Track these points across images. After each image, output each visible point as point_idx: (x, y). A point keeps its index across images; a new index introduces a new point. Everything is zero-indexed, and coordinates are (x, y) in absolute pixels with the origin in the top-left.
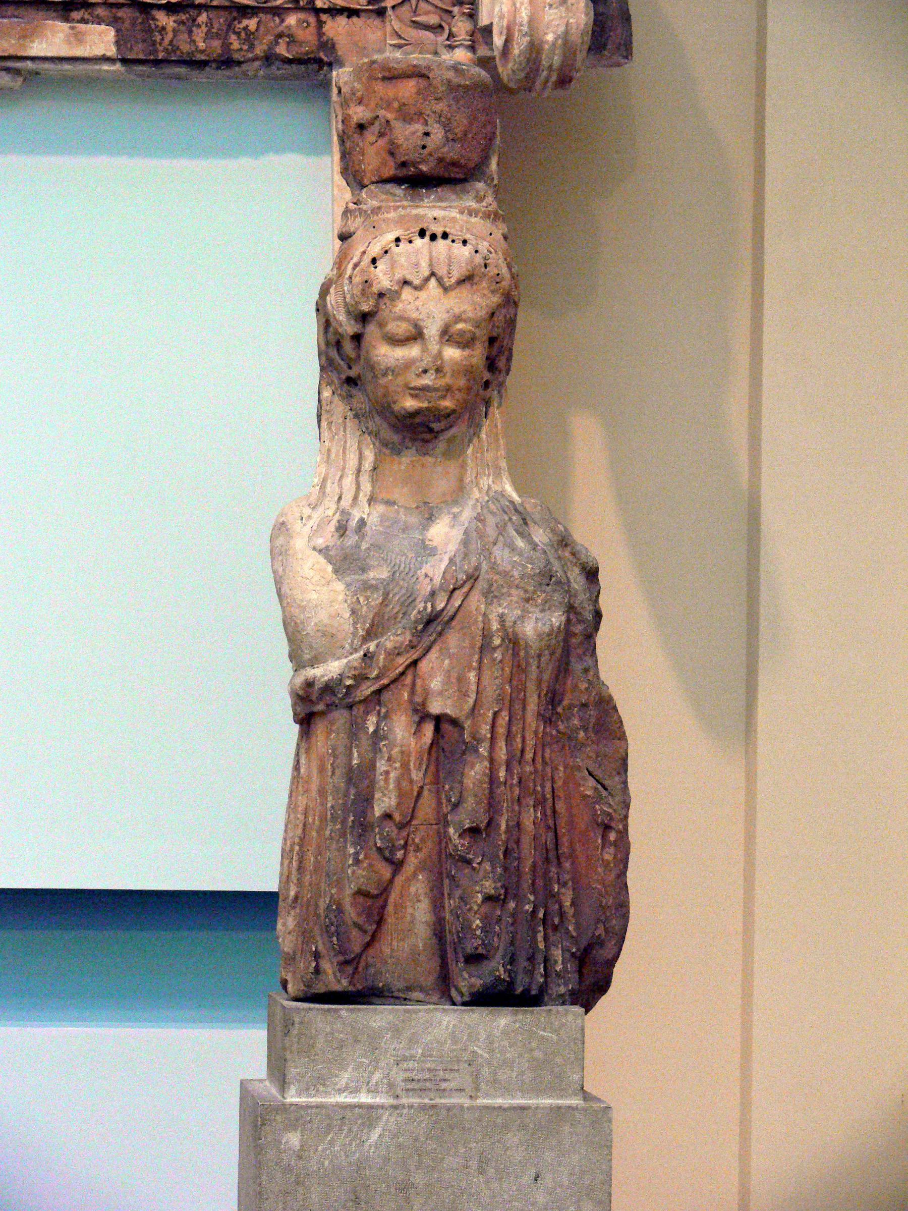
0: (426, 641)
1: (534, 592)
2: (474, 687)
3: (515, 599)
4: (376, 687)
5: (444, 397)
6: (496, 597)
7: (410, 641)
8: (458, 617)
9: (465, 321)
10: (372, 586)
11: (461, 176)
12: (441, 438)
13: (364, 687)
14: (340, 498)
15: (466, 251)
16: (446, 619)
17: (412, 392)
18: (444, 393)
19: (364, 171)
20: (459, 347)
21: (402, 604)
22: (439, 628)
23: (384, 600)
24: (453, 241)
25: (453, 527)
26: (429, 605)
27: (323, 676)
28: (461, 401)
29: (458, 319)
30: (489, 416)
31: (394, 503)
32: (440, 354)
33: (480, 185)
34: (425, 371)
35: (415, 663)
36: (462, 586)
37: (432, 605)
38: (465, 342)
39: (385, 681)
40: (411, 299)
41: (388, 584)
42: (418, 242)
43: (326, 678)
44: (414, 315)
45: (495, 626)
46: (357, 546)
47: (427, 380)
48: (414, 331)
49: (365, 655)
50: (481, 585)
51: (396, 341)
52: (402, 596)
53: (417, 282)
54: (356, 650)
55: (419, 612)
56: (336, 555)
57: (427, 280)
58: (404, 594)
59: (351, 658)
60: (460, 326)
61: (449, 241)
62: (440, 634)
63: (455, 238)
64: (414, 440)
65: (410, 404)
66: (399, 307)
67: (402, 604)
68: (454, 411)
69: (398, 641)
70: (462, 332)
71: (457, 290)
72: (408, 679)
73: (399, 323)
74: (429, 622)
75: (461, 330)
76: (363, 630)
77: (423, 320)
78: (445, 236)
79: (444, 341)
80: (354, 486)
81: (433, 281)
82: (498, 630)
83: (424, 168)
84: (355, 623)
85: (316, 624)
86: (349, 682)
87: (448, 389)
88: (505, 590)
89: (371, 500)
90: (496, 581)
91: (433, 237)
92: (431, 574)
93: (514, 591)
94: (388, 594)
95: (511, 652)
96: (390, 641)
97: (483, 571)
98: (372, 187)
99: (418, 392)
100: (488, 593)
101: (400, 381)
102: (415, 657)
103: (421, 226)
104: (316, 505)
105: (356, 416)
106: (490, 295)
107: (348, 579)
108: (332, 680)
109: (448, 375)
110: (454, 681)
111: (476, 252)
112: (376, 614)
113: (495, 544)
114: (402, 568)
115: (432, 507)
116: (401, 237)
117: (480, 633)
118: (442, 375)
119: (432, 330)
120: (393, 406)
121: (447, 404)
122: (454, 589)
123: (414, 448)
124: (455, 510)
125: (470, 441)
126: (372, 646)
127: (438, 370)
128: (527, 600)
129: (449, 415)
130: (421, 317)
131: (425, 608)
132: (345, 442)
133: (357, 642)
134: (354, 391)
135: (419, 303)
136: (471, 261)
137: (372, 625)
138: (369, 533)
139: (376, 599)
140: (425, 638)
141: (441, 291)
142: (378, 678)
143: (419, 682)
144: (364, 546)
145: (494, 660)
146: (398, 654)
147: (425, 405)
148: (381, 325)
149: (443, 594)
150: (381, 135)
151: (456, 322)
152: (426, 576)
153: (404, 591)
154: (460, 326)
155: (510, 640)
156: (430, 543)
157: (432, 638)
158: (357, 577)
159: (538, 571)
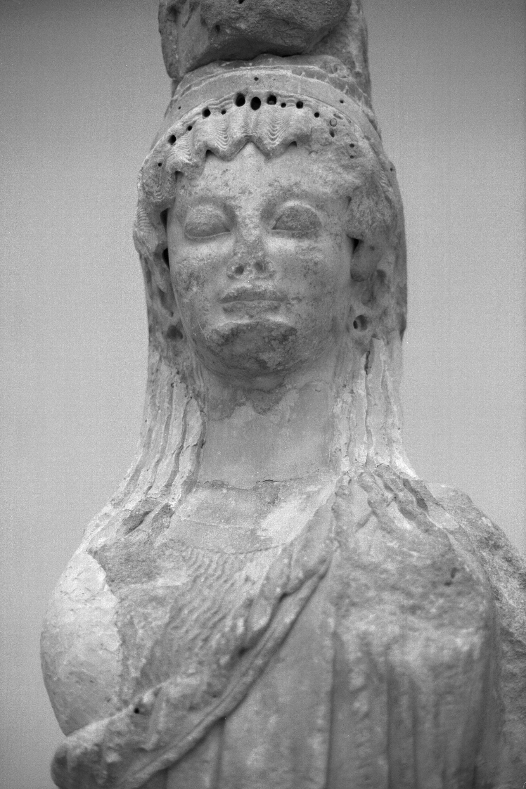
0: (235, 686)
1: (424, 596)
2: (320, 763)
3: (389, 608)
4: (156, 765)
5: (275, 309)
6: (354, 604)
7: (209, 685)
8: (292, 641)
9: (297, 197)
10: (154, 599)
11: (298, 42)
12: (289, 386)
13: (137, 765)
14: (150, 488)
15: (300, 112)
16: (270, 645)
17: (226, 305)
18: (275, 303)
19: (179, 61)
20: (293, 236)
21: (203, 626)
22: (259, 662)
23: (172, 619)
24: (283, 105)
25: (302, 510)
26: (240, 623)
27: (75, 748)
28: (304, 316)
29: (288, 193)
30: (372, 370)
31: (222, 485)
32: (258, 244)
33: (329, 58)
34: (240, 270)
35: (221, 722)
36: (297, 589)
37: (246, 622)
38: (302, 227)
39: (171, 755)
40: (218, 173)
41: (183, 595)
42: (234, 108)
43: (78, 751)
44: (221, 193)
45: (353, 653)
46: (149, 542)
47: (244, 283)
48: (223, 217)
49: (137, 711)
50: (330, 585)
51: (198, 235)
52: (205, 612)
53: (222, 146)
54: (126, 703)
55: (223, 636)
56: (114, 557)
57: (240, 145)
58: (209, 609)
59: (118, 715)
60: (291, 203)
61: (278, 106)
62: (261, 672)
63: (285, 100)
64: (249, 391)
65: (223, 323)
66: (201, 185)
67: (203, 626)
68: (292, 331)
69: (188, 685)
70: (294, 213)
71: (286, 157)
72: (210, 752)
73: (201, 207)
74: (242, 651)
75: (292, 208)
76: (136, 669)
77: (234, 198)
78: (272, 99)
79: (269, 228)
80: (171, 468)
81: (249, 149)
82: (358, 661)
83: (243, 26)
84: (125, 659)
85: (70, 663)
86: (112, 757)
87: (279, 301)
88: (371, 593)
89: (191, 485)
90: (354, 580)
91: (256, 104)
92: (254, 577)
93: (386, 595)
94: (180, 610)
95: (384, 698)
96: (176, 686)
97: (334, 563)
98: (187, 76)
99: (233, 302)
100: (341, 597)
101: (209, 291)
102: (219, 712)
103: (237, 90)
104: (122, 500)
105: (184, 379)
106: (340, 170)
107: (125, 590)
108: (85, 753)
109: (278, 276)
110: (285, 751)
111: (317, 115)
112: (157, 643)
113: (361, 525)
114: (210, 571)
115: (277, 487)
116: (210, 107)
117: (329, 667)
118: (265, 275)
119: (249, 210)
120: (203, 332)
121: (279, 319)
122: (284, 596)
123: (249, 403)
124: (312, 488)
125: (338, 395)
126: (147, 697)
127: (260, 267)
128: (413, 610)
129: (284, 338)
130: (231, 194)
131: (234, 628)
132: (170, 417)
133: (127, 690)
134: (179, 344)
135: (228, 176)
136: (307, 121)
137: (150, 661)
138: (173, 525)
139: (160, 616)
140: (234, 681)
141: (262, 158)
142: (158, 748)
143: (227, 756)
144: (159, 541)
145: (355, 713)
146: (192, 708)
147: (245, 321)
148: (181, 218)
149: (264, 602)
150: (193, 8)
151: (285, 199)
152: (247, 579)
153: (208, 604)
154: (291, 203)
155: (381, 678)
156: (264, 533)
157: (248, 679)
158: (138, 586)
159: (429, 562)
